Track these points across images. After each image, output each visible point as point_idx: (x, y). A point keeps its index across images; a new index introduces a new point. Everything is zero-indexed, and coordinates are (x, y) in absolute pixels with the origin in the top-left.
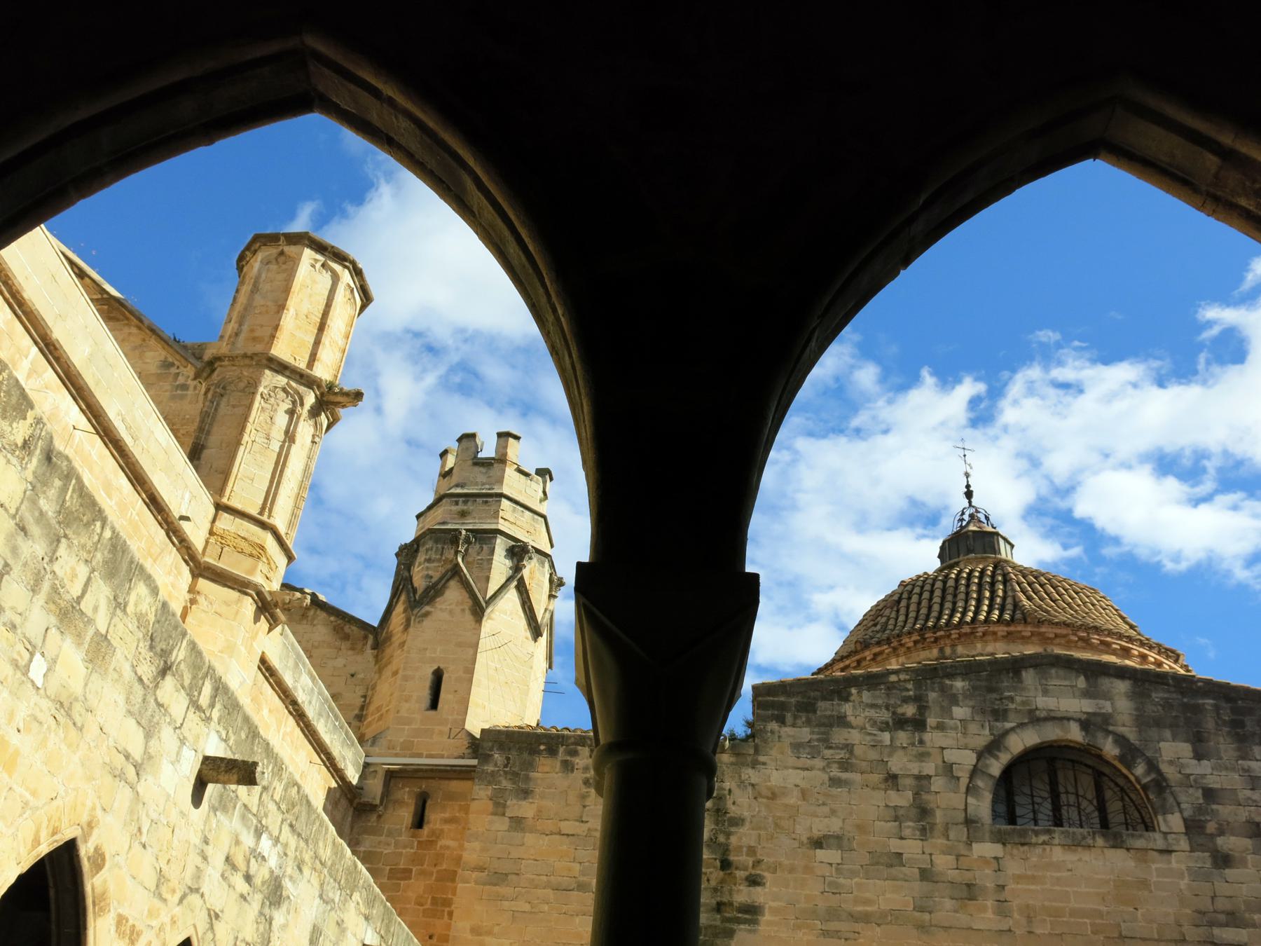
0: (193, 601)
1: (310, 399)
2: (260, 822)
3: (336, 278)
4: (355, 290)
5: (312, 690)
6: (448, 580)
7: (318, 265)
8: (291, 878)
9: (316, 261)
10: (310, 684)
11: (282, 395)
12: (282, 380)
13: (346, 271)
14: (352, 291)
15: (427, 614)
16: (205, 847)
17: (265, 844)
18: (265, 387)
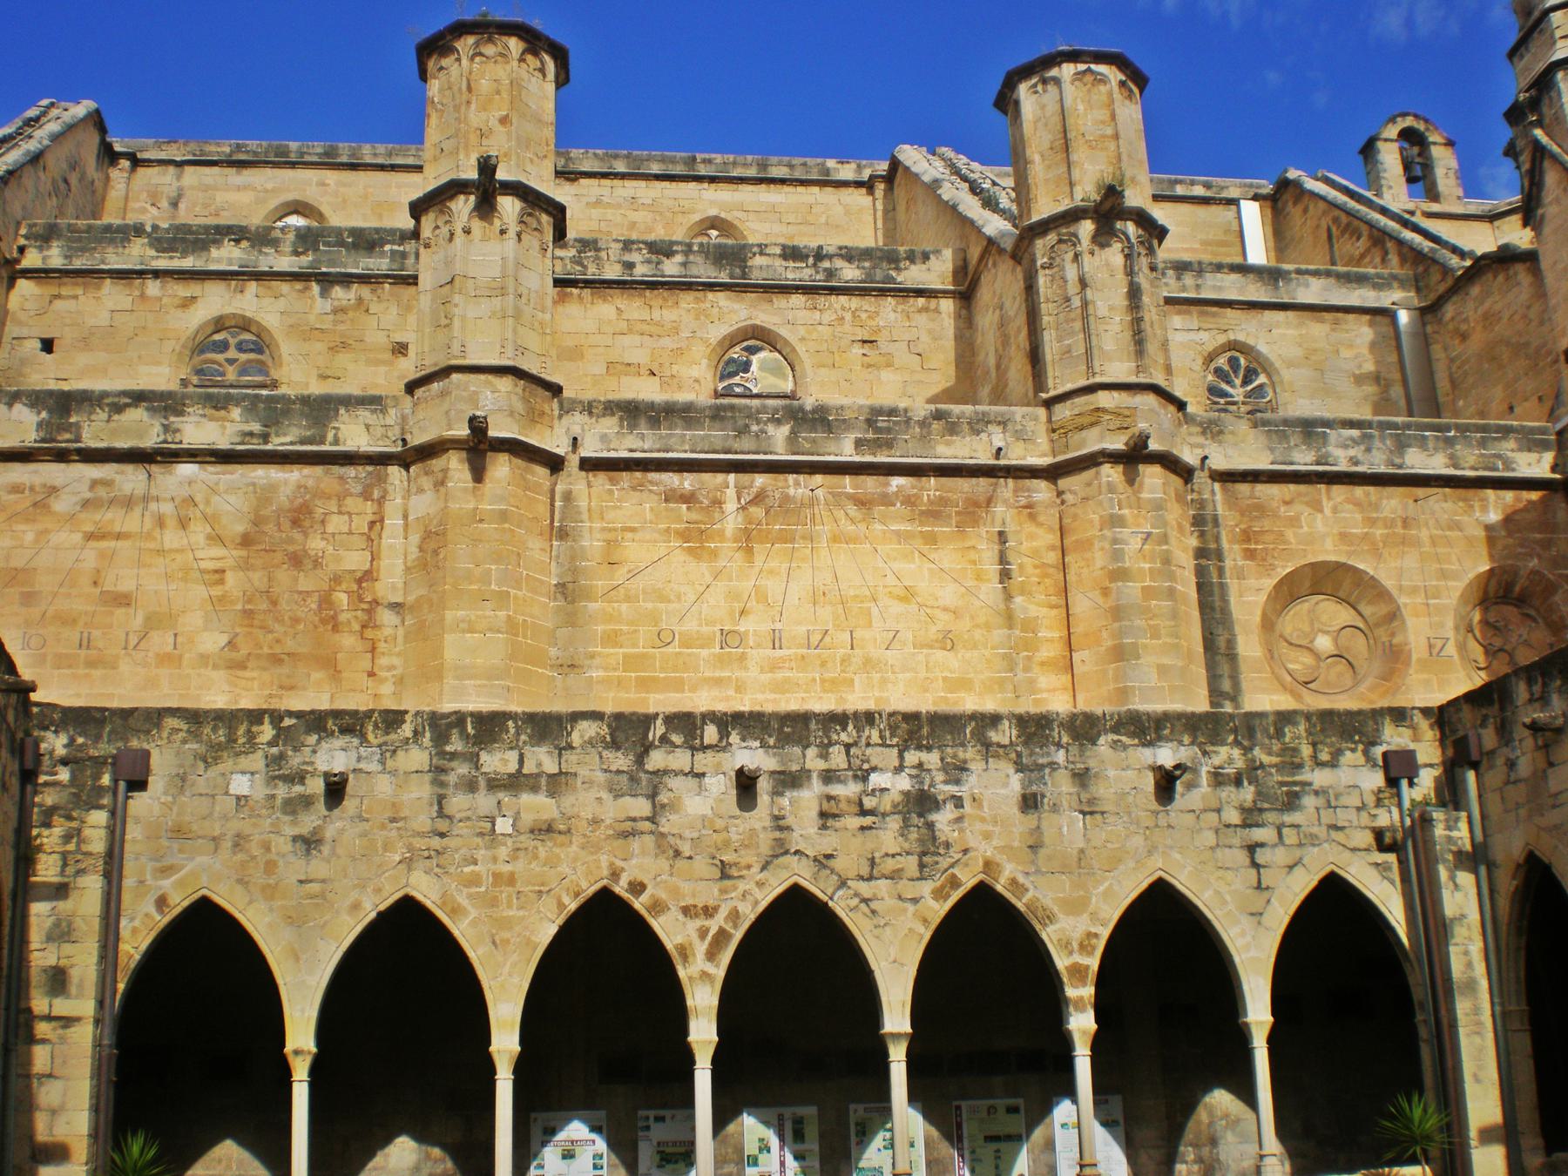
0: (1063, 502)
1: (1087, 228)
2: (861, 769)
3: (1057, 81)
4: (1093, 66)
5: (1364, 436)
6: (1541, 163)
7: (1040, 88)
8: (946, 782)
9: (1035, 85)
10: (1355, 433)
11: (1063, 246)
12: (1052, 238)
13: (1065, 66)
14: (1089, 70)
15: (1542, 217)
16: (781, 823)
17: (876, 780)
18: (1043, 256)
